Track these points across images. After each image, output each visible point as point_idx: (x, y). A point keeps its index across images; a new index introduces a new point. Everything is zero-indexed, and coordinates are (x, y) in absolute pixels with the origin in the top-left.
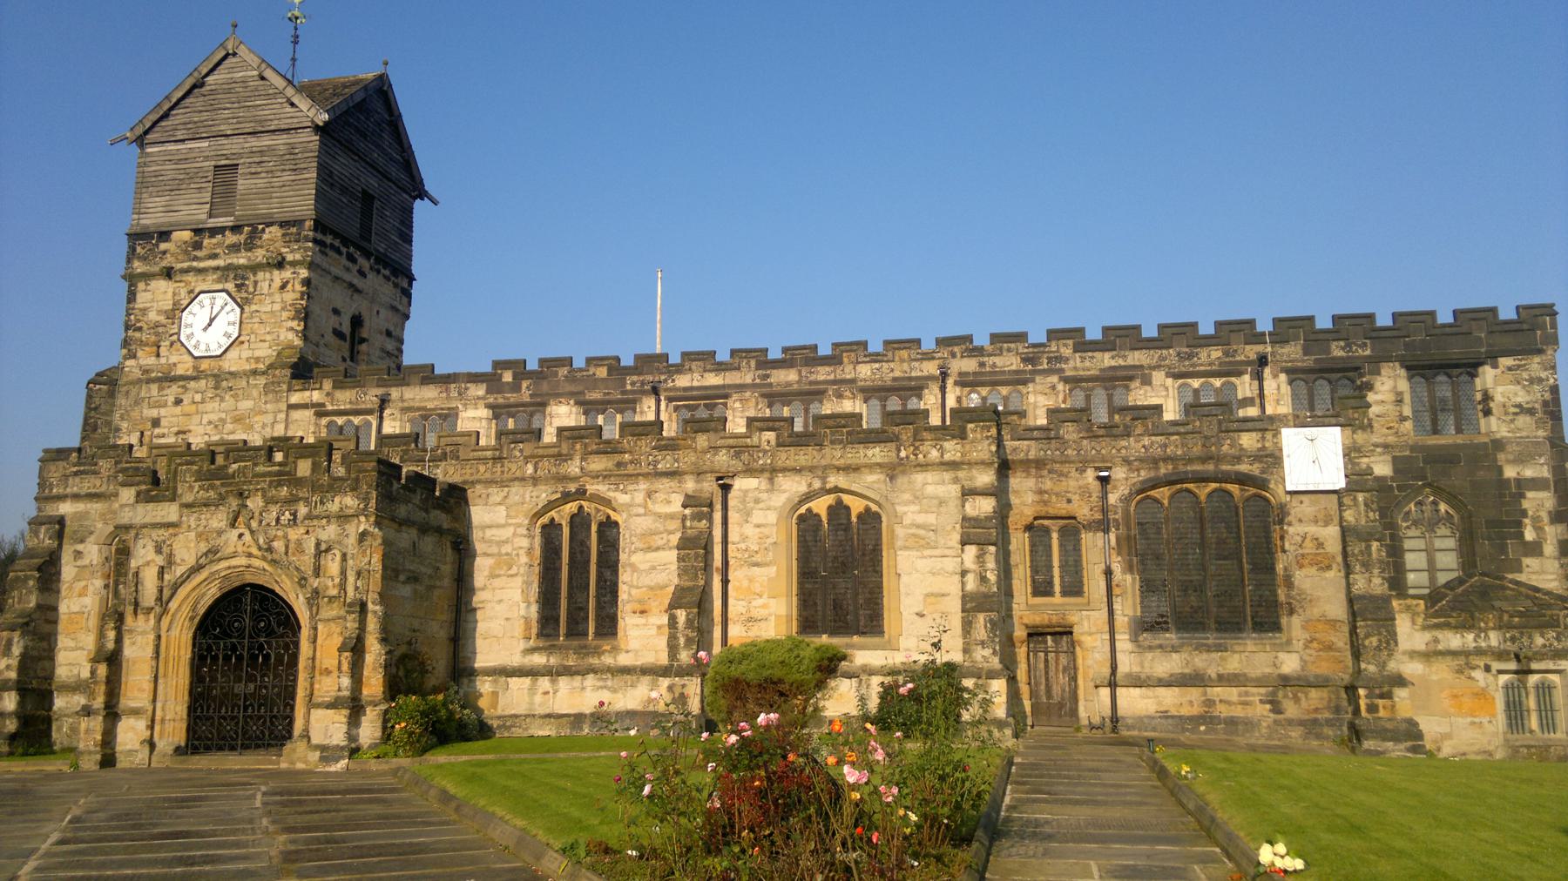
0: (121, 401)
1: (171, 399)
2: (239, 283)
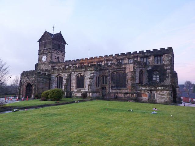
2: (46, 54)
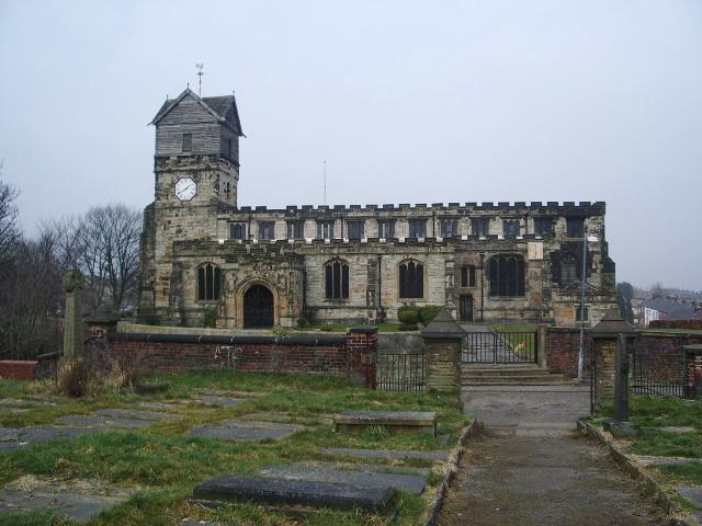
0: (157, 215)
2: (195, 175)
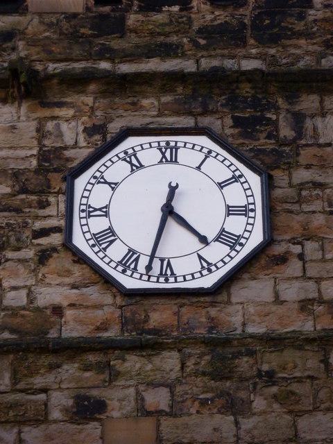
1: (60, 401)
